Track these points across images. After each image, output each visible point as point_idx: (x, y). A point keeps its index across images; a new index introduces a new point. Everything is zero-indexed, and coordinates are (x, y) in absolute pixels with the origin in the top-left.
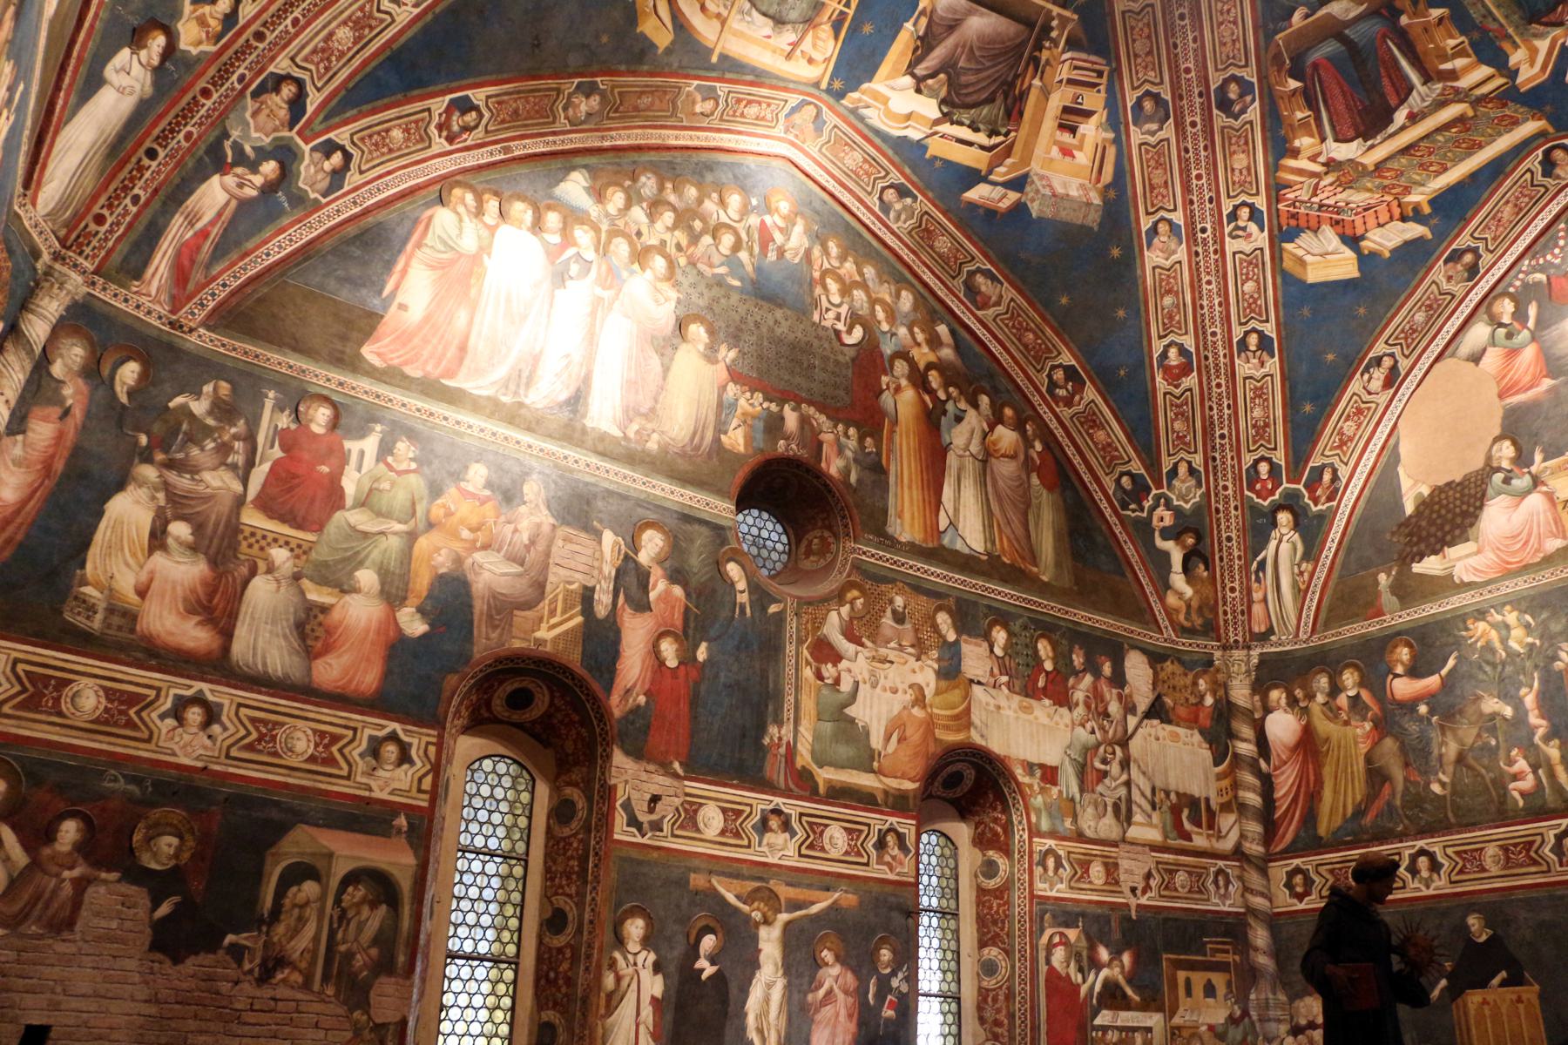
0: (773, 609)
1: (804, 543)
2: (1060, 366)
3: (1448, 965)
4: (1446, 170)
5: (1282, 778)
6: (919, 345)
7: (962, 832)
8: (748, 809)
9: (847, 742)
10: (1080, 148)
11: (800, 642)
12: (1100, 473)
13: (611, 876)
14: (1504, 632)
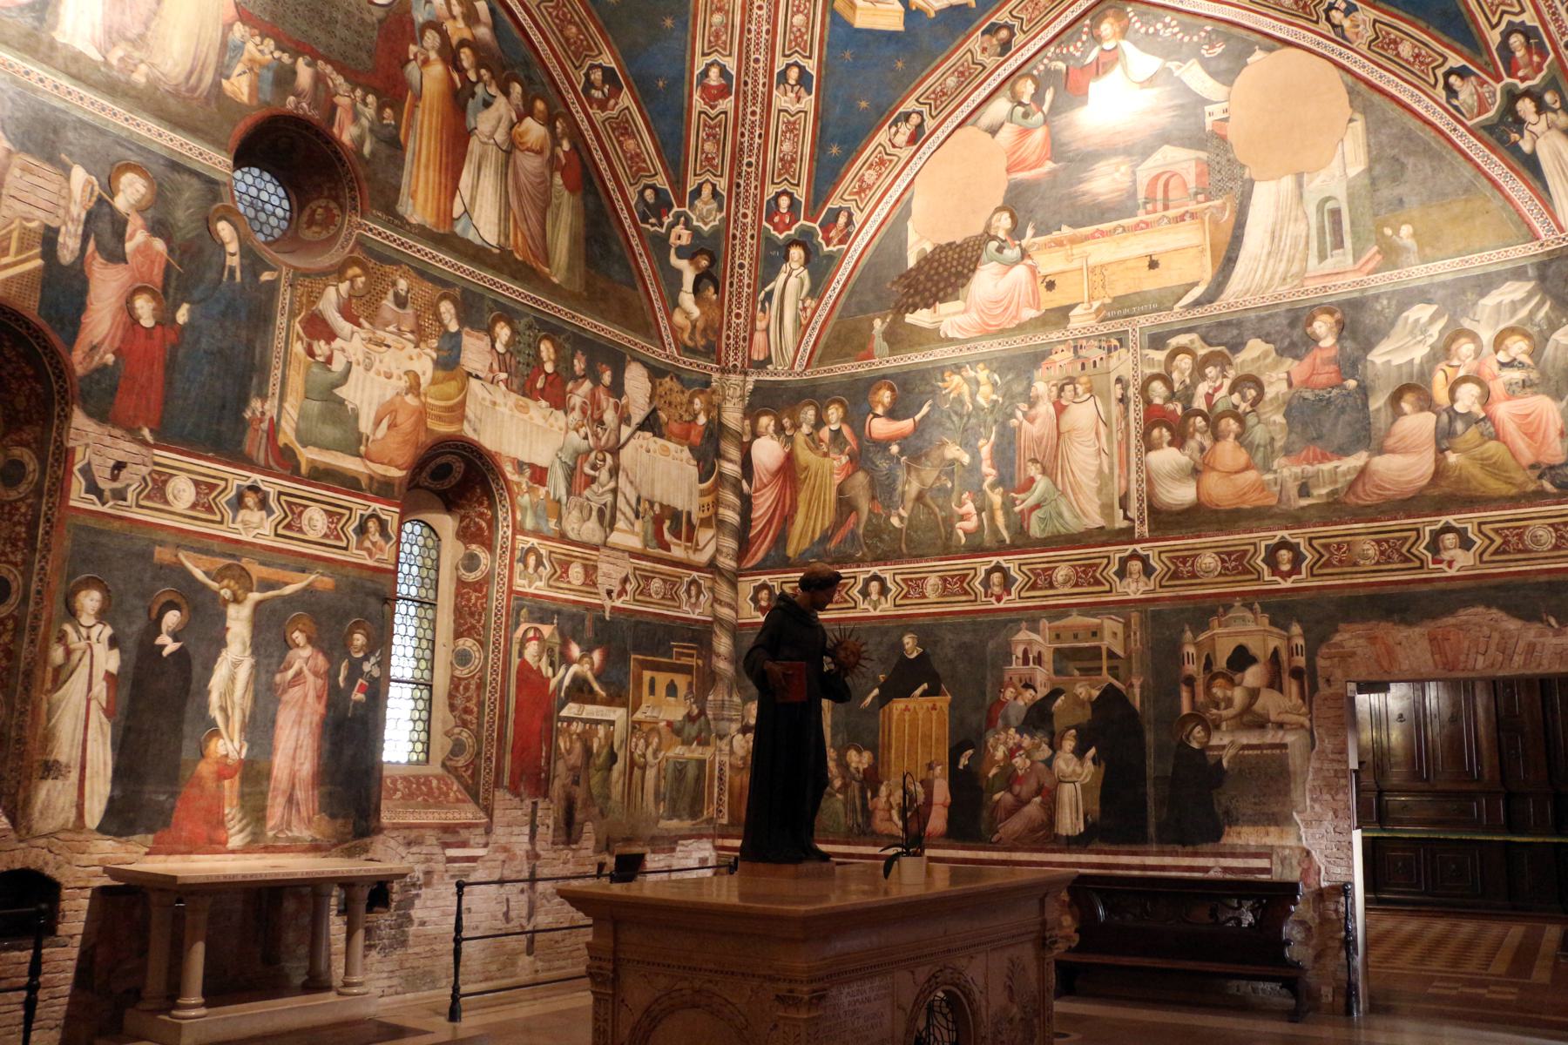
0: (266, 276)
1: (307, 212)
2: (600, 66)
3: (882, 677)
5: (762, 499)
6: (454, 18)
7: (447, 524)
8: (223, 484)
9: (334, 423)
11: (293, 315)
12: (625, 182)
13: (64, 544)
14: (974, 387)
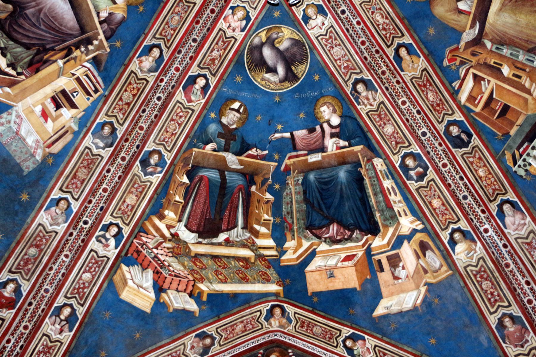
10: (54, 120)
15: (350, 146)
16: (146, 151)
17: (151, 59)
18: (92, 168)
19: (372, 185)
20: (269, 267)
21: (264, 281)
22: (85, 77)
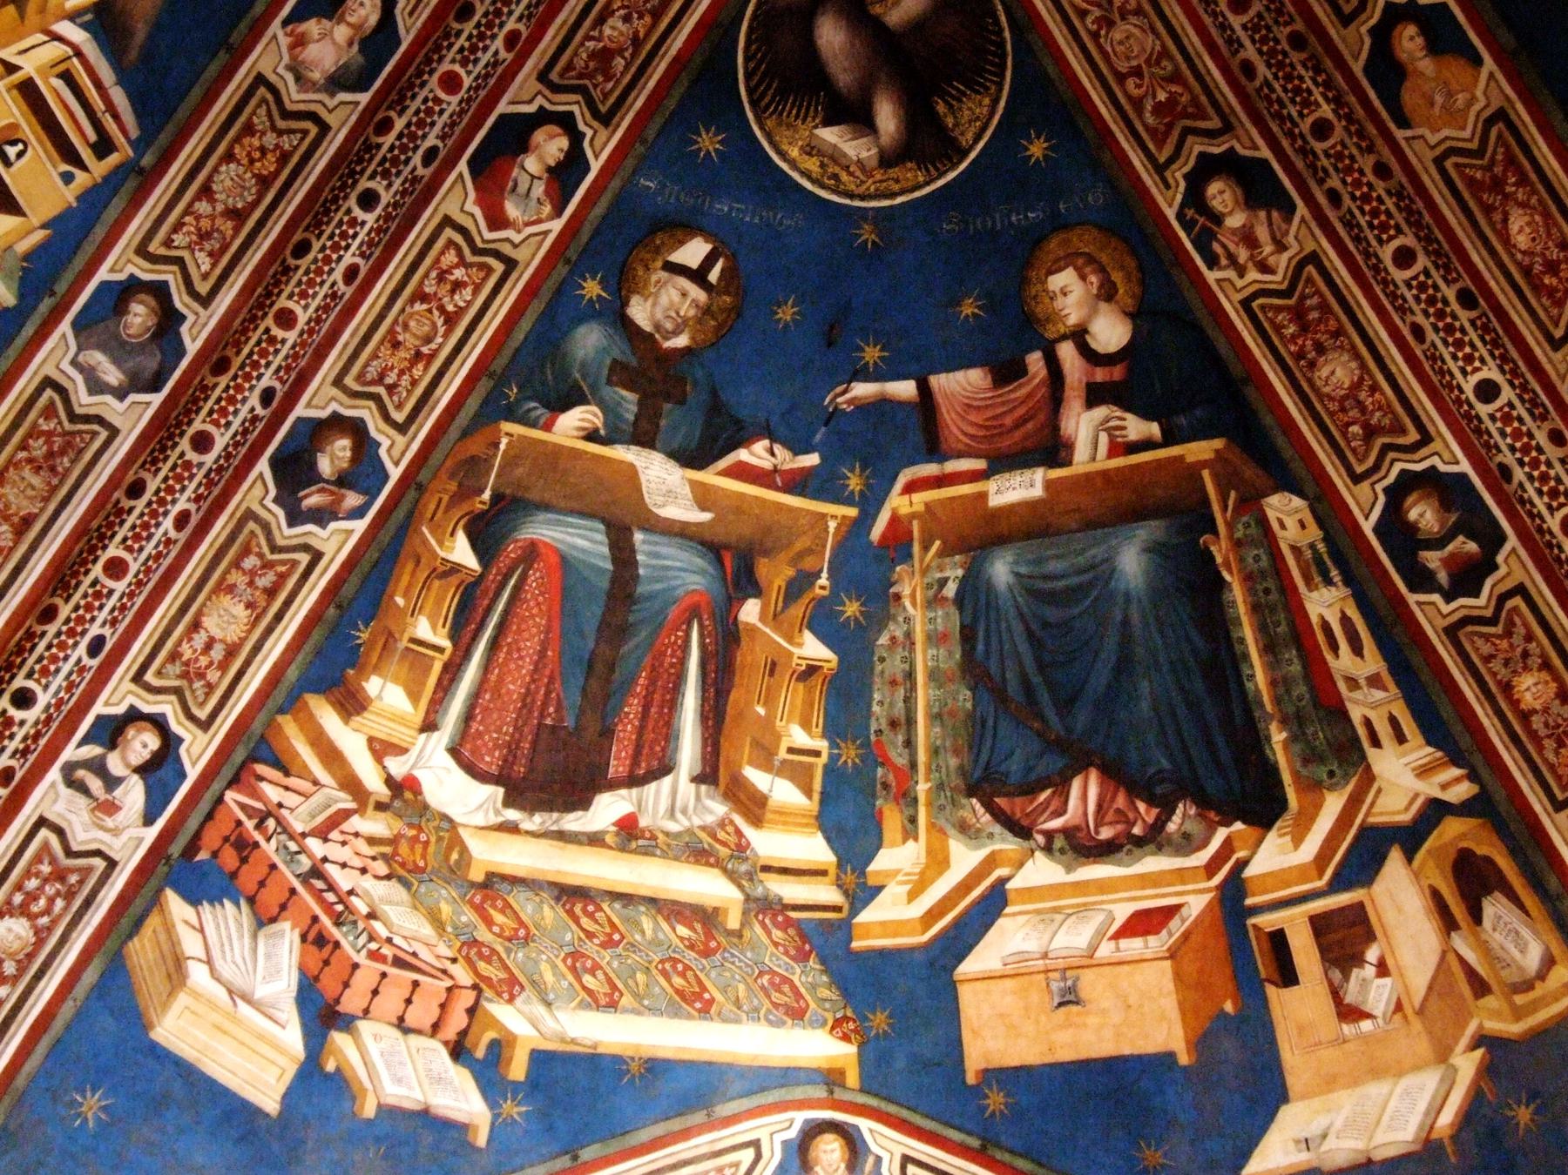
4: (612, 1005)
15: (1169, 439)
16: (299, 419)
17: (342, 33)
18: (68, 471)
19: (1255, 608)
20: (802, 957)
21: (780, 1013)
22: (59, 84)
